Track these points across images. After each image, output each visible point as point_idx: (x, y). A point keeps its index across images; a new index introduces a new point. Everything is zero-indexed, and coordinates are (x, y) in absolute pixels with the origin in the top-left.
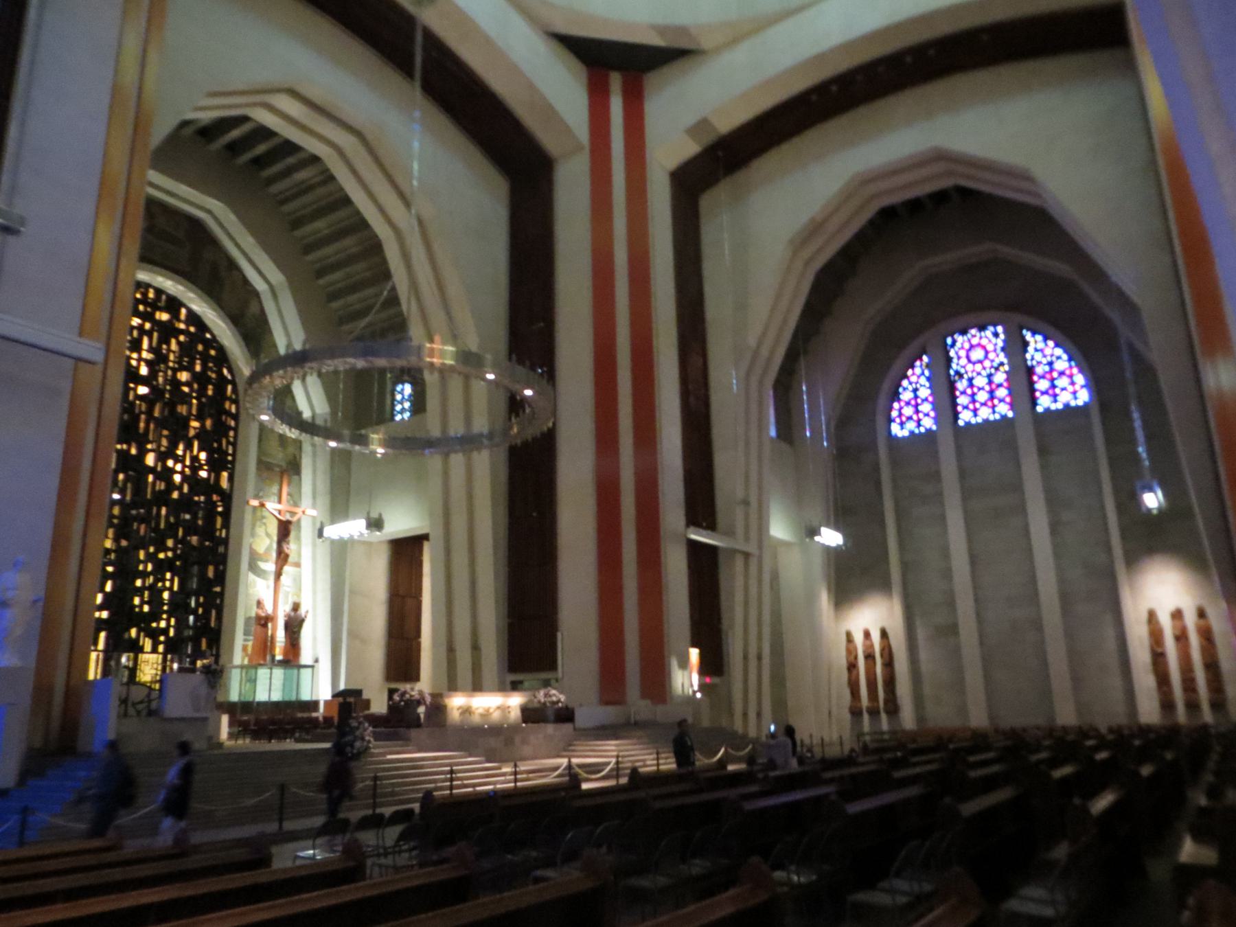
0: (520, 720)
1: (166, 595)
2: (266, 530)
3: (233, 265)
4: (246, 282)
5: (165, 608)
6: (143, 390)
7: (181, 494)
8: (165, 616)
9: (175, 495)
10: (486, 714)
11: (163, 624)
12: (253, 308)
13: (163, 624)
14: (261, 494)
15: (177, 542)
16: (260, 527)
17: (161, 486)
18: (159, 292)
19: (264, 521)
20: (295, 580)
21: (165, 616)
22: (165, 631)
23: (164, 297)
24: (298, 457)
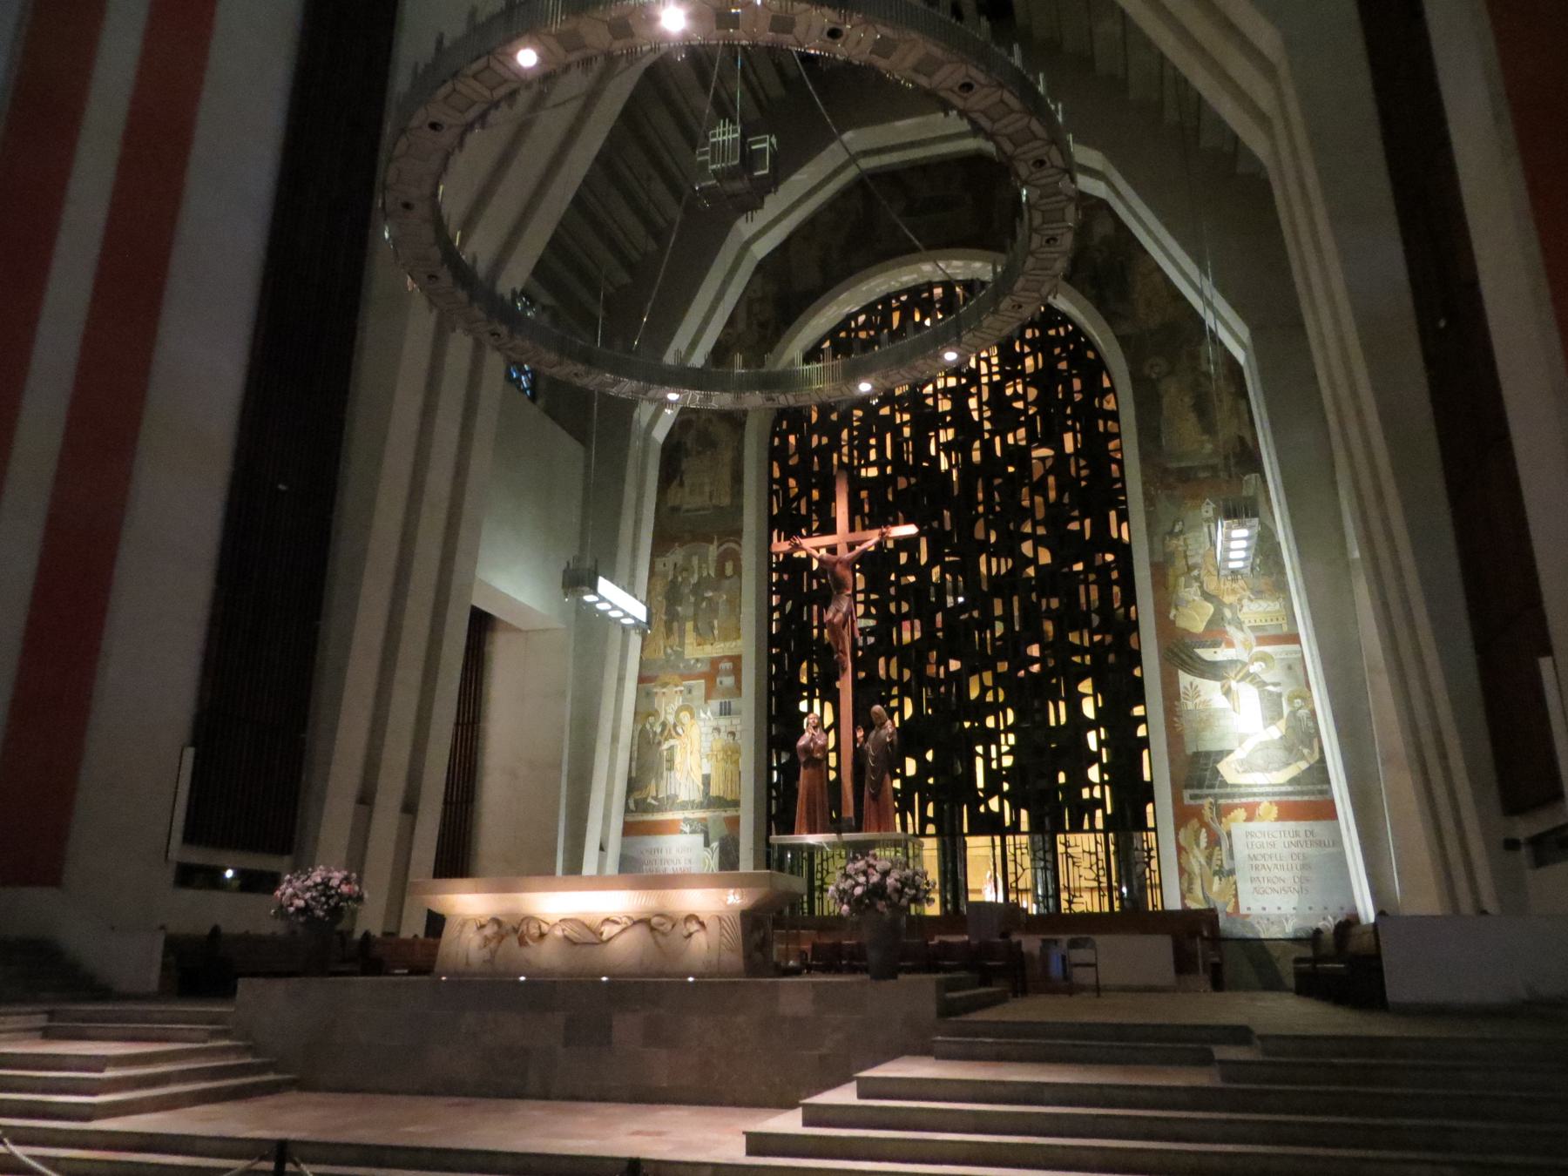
0: (735, 959)
2: (1201, 587)
6: (947, 435)
7: (1039, 569)
10: (585, 937)
14: (1177, 529)
17: (1005, 565)
18: (948, 285)
19: (1195, 573)
24: (1248, 438)
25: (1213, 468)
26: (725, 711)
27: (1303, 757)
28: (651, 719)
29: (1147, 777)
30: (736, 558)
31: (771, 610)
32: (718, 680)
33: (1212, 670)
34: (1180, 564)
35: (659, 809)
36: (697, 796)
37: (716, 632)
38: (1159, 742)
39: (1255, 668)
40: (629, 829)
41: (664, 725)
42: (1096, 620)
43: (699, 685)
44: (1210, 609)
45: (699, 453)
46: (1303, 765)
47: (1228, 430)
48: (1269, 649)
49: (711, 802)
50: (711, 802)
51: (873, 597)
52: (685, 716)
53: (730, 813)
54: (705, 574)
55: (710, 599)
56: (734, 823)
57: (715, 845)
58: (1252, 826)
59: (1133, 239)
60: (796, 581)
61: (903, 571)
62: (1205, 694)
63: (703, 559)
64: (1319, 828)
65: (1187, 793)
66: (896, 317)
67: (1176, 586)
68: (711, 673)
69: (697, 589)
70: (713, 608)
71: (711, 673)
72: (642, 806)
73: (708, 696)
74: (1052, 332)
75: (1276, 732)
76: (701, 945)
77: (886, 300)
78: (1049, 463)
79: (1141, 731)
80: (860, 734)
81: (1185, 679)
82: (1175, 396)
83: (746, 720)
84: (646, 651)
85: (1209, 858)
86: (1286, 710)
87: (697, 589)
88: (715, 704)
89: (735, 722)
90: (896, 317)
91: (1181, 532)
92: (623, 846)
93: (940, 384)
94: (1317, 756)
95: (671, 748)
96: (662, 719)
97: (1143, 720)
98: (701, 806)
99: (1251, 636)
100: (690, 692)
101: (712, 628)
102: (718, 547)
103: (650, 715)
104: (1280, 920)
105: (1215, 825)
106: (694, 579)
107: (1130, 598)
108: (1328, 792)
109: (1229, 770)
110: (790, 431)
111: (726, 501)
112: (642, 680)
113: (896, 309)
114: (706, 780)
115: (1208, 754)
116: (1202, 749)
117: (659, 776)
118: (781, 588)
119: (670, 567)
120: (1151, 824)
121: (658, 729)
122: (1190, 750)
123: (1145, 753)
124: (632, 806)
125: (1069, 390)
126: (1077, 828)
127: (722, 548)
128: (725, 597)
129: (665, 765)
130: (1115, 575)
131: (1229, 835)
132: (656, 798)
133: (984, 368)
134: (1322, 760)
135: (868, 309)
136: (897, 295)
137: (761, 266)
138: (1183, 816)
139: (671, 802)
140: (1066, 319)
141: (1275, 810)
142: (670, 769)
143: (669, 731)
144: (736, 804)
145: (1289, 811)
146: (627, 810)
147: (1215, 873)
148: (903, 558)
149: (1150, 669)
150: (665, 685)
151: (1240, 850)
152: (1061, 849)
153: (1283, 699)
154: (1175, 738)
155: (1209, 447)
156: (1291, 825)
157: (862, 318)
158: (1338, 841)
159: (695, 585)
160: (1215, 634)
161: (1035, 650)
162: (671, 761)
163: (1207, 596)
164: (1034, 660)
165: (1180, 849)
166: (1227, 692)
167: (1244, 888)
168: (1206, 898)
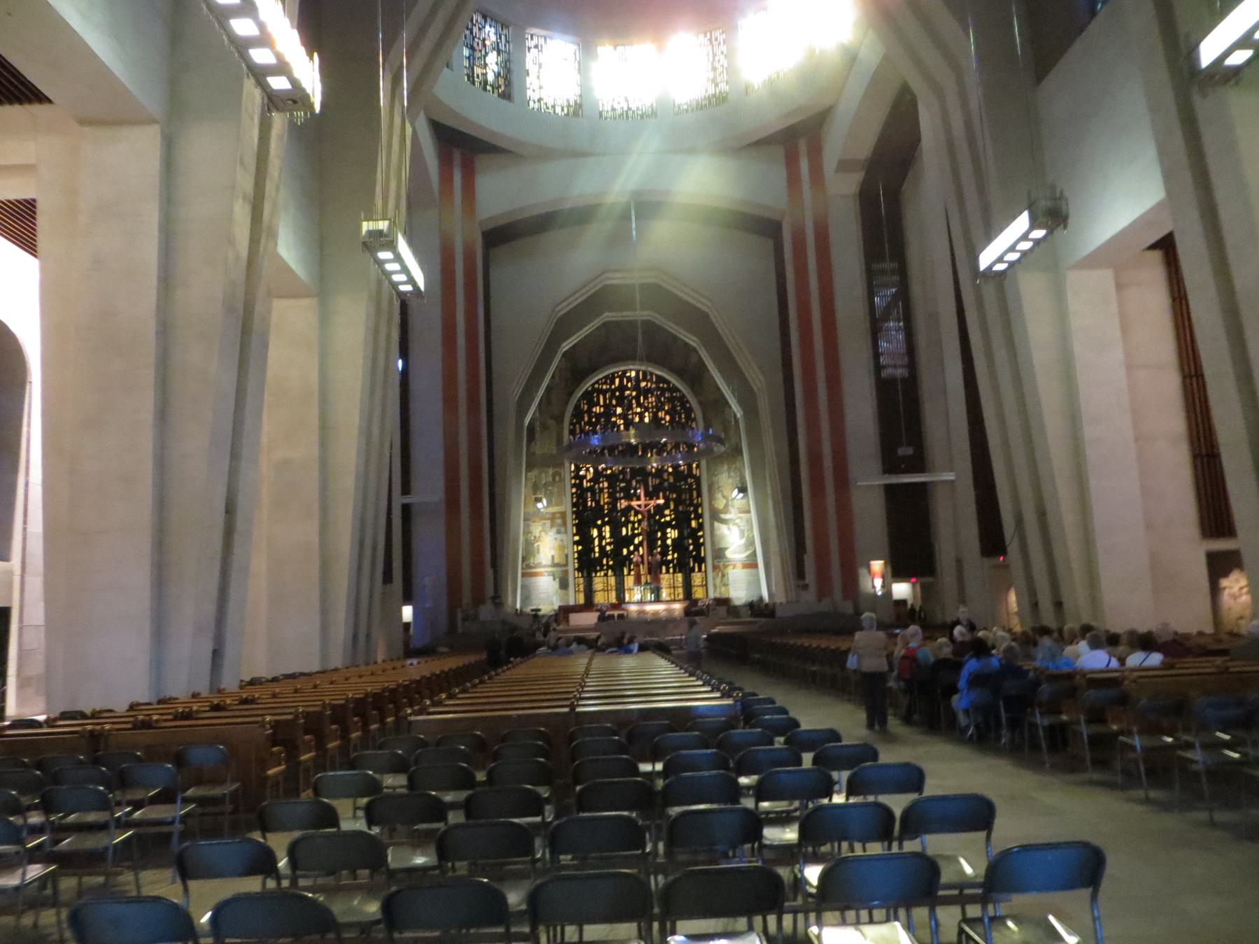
0: (683, 614)
1: (669, 542)
5: (670, 548)
7: (669, 483)
8: (670, 553)
9: (666, 484)
10: (656, 613)
11: (670, 557)
12: (694, 360)
13: (670, 557)
15: (671, 511)
16: (718, 493)
19: (721, 489)
21: (670, 553)
22: (672, 561)
23: (641, 373)
26: (559, 532)
27: (750, 550)
28: (530, 535)
29: (703, 555)
31: (573, 494)
33: (724, 522)
34: (716, 486)
36: (549, 563)
37: (554, 502)
38: (708, 545)
39: (738, 521)
40: (524, 575)
41: (535, 537)
42: (688, 502)
43: (548, 523)
44: (725, 501)
46: (748, 553)
48: (742, 515)
49: (554, 565)
50: (554, 565)
51: (611, 490)
52: (543, 534)
53: (563, 569)
55: (550, 490)
56: (566, 572)
57: (558, 580)
58: (734, 570)
60: (581, 483)
61: (622, 481)
62: (722, 529)
66: (617, 381)
67: (714, 493)
68: (553, 518)
70: (552, 493)
71: (553, 518)
72: (529, 567)
73: (552, 526)
74: (674, 394)
75: (743, 541)
76: (677, 613)
77: (613, 374)
78: (673, 444)
79: (701, 540)
80: (650, 558)
81: (716, 524)
83: (571, 535)
88: (554, 530)
89: (563, 537)
90: (617, 381)
92: (522, 581)
93: (634, 411)
95: (538, 546)
96: (534, 534)
97: (702, 536)
98: (548, 566)
99: (737, 511)
100: (544, 524)
103: (529, 533)
104: (741, 599)
106: (544, 482)
107: (699, 495)
108: (756, 560)
109: (729, 554)
110: (577, 423)
111: (554, 452)
112: (524, 520)
113: (617, 377)
114: (553, 557)
116: (721, 547)
117: (534, 556)
118: (574, 486)
119: (533, 477)
120: (703, 569)
121: (533, 538)
122: (717, 547)
123: (702, 548)
124: (524, 566)
125: (680, 418)
126: (679, 572)
129: (536, 552)
130: (694, 487)
131: (728, 574)
132: (534, 563)
133: (650, 405)
134: (755, 551)
135: (606, 377)
136: (617, 372)
137: (565, 355)
138: (715, 568)
139: (539, 565)
140: (678, 390)
141: (741, 566)
142: (538, 553)
143: (536, 539)
144: (566, 565)
146: (522, 568)
147: (723, 585)
148: (621, 477)
150: (534, 522)
151: (730, 576)
152: (675, 578)
153: (746, 532)
154: (713, 543)
156: (746, 570)
157: (604, 380)
158: (758, 575)
159: (545, 484)
160: (726, 510)
161: (667, 512)
162: (538, 550)
163: (724, 497)
164: (667, 516)
165: (714, 579)
166: (729, 529)
168: (720, 593)
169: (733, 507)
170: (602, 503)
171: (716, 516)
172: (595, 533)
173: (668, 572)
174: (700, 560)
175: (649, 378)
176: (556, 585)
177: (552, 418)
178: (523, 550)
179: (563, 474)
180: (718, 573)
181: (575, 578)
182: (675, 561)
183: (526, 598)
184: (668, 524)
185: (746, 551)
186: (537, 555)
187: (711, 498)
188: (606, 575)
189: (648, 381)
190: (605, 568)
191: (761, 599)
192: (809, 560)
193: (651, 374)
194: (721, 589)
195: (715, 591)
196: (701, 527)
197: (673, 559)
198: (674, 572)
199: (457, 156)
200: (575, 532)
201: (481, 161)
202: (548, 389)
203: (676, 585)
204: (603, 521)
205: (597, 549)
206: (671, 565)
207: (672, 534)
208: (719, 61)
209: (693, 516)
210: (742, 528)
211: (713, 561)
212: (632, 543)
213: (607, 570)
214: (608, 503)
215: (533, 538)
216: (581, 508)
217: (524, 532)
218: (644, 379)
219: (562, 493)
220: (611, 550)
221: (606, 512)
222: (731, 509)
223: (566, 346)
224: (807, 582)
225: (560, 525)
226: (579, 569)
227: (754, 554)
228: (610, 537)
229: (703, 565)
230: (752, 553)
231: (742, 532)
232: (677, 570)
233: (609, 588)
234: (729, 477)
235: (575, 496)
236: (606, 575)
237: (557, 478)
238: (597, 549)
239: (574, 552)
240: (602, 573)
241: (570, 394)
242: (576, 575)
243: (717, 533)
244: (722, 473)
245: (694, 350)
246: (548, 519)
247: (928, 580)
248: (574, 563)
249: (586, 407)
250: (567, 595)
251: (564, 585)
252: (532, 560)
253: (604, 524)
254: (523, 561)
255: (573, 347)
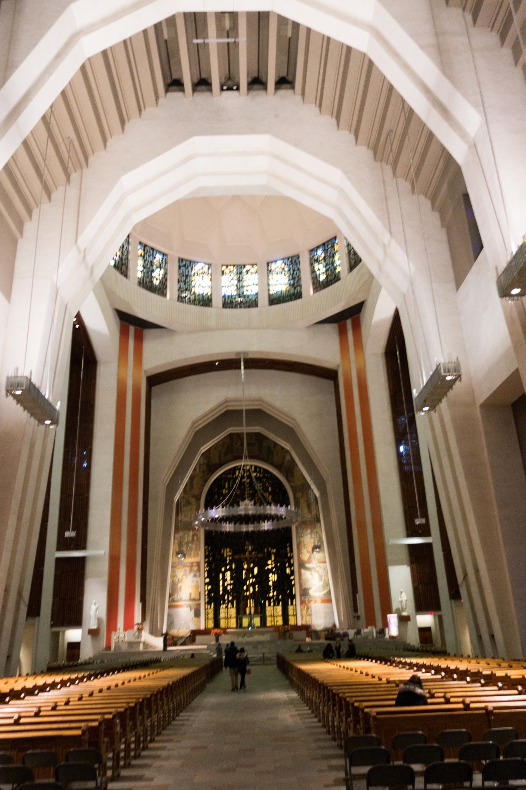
1: (271, 583)
3: (276, 444)
4: (283, 448)
8: (272, 591)
12: (288, 458)
13: (271, 595)
14: (302, 535)
15: (272, 562)
16: (304, 549)
19: (306, 546)
20: (324, 569)
23: (253, 467)
25: (311, 522)
26: (195, 576)
30: (197, 535)
31: (205, 550)
32: (193, 568)
34: (302, 544)
35: (178, 601)
37: (192, 555)
38: (297, 585)
39: (317, 569)
40: (170, 607)
42: (284, 555)
43: (188, 569)
44: (308, 555)
45: (186, 506)
46: (326, 591)
47: (314, 513)
49: (192, 600)
50: (192, 600)
53: (197, 602)
54: (189, 540)
56: (199, 605)
57: (193, 611)
59: (294, 461)
63: (188, 535)
64: (329, 605)
65: (302, 598)
67: (301, 549)
69: (187, 543)
70: (191, 549)
71: (191, 566)
72: (173, 601)
73: (190, 572)
75: (321, 583)
79: (293, 583)
81: (303, 571)
82: (302, 501)
84: (174, 559)
85: (307, 612)
86: (323, 579)
87: (187, 543)
89: (198, 579)
91: (303, 536)
92: (168, 611)
94: (329, 589)
95: (181, 586)
97: (294, 579)
101: (191, 554)
102: (193, 532)
105: (308, 605)
106: (186, 540)
107: (291, 551)
109: (311, 592)
112: (172, 567)
114: (190, 594)
115: (307, 589)
117: (178, 594)
120: (294, 603)
122: (303, 587)
127: (194, 532)
128: (194, 546)
131: (311, 607)
134: (330, 590)
138: (302, 602)
139: (181, 600)
141: (320, 601)
144: (200, 599)
145: (324, 601)
146: (169, 602)
149: (296, 567)
151: (313, 610)
153: (323, 576)
154: (301, 585)
155: (309, 516)
158: (332, 608)
160: (309, 561)
163: (308, 552)
165: (301, 610)
166: (312, 574)
167: (313, 617)
168: (306, 621)
169: (315, 559)
170: (225, 555)
171: (302, 565)
172: (221, 576)
173: (270, 605)
174: (293, 597)
175: (258, 470)
176: (192, 613)
177: (193, 496)
178: (170, 589)
179: (199, 535)
180: (304, 606)
181: (205, 609)
182: (275, 598)
183: (171, 624)
184: (270, 571)
185: (323, 590)
186: (179, 592)
187: (299, 553)
188: (227, 607)
189: (257, 473)
190: (226, 602)
191: (334, 626)
192: (360, 596)
193: (260, 468)
194: (306, 618)
195: (302, 619)
196: (292, 573)
197: (273, 595)
198: (274, 605)
199: (132, 329)
200: (206, 575)
201: (148, 333)
202: (192, 478)
203: (275, 615)
204: (226, 568)
205: (221, 588)
206: (272, 600)
207: (273, 578)
208: (296, 274)
209: (287, 565)
210: (321, 574)
211: (301, 599)
212: (246, 584)
213: (228, 603)
214: (230, 556)
215: (177, 580)
216: (211, 559)
217: (171, 576)
218: (255, 471)
219: (198, 549)
220: (231, 589)
221: (228, 562)
222: (313, 560)
223: (204, 449)
224: (359, 614)
225: (195, 571)
226: (209, 603)
227: (329, 592)
228: (231, 580)
229: (294, 600)
230: (327, 592)
231: (321, 577)
232: (276, 604)
233: (229, 616)
234: (311, 538)
235: (207, 550)
236: (227, 607)
237: (195, 538)
238: (221, 588)
239: (205, 591)
240: (224, 606)
241: (206, 481)
242: (206, 607)
243: (303, 577)
244: (306, 535)
245: (288, 451)
246: (188, 566)
247: (439, 613)
248: (205, 599)
249: (216, 490)
250: (199, 622)
251: (197, 614)
252: (176, 595)
253: (226, 570)
254: (170, 597)
255: (209, 450)
